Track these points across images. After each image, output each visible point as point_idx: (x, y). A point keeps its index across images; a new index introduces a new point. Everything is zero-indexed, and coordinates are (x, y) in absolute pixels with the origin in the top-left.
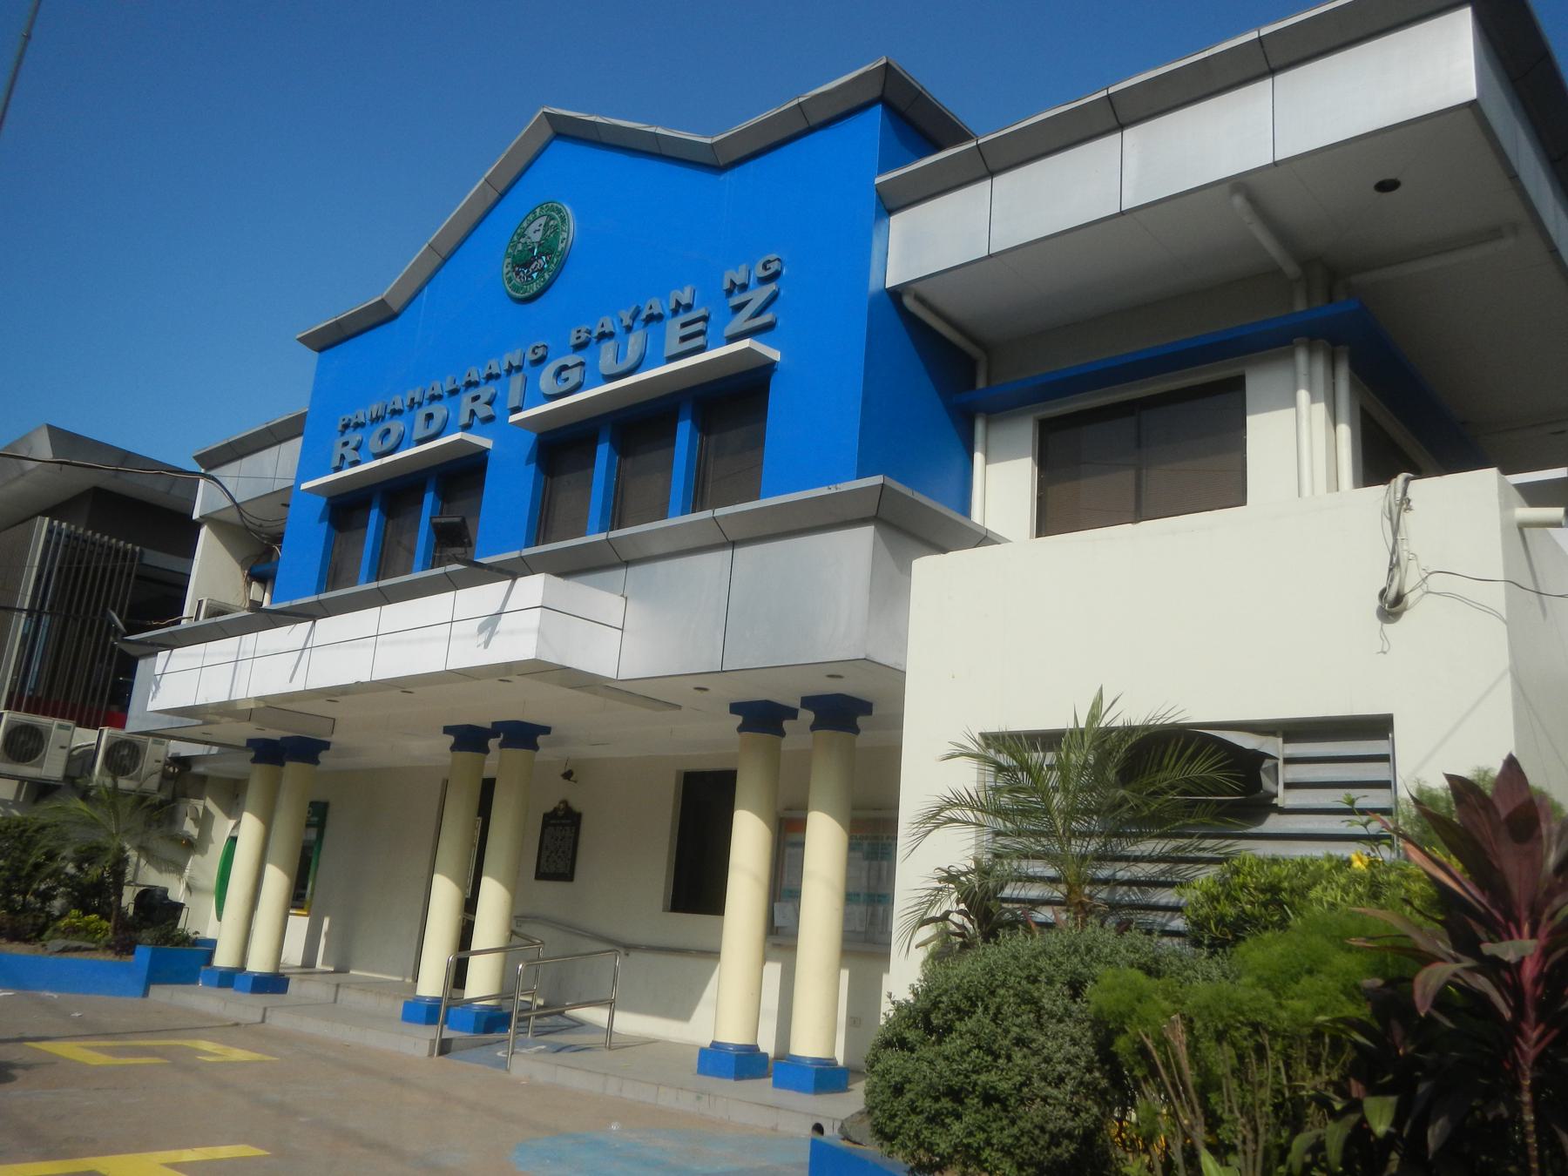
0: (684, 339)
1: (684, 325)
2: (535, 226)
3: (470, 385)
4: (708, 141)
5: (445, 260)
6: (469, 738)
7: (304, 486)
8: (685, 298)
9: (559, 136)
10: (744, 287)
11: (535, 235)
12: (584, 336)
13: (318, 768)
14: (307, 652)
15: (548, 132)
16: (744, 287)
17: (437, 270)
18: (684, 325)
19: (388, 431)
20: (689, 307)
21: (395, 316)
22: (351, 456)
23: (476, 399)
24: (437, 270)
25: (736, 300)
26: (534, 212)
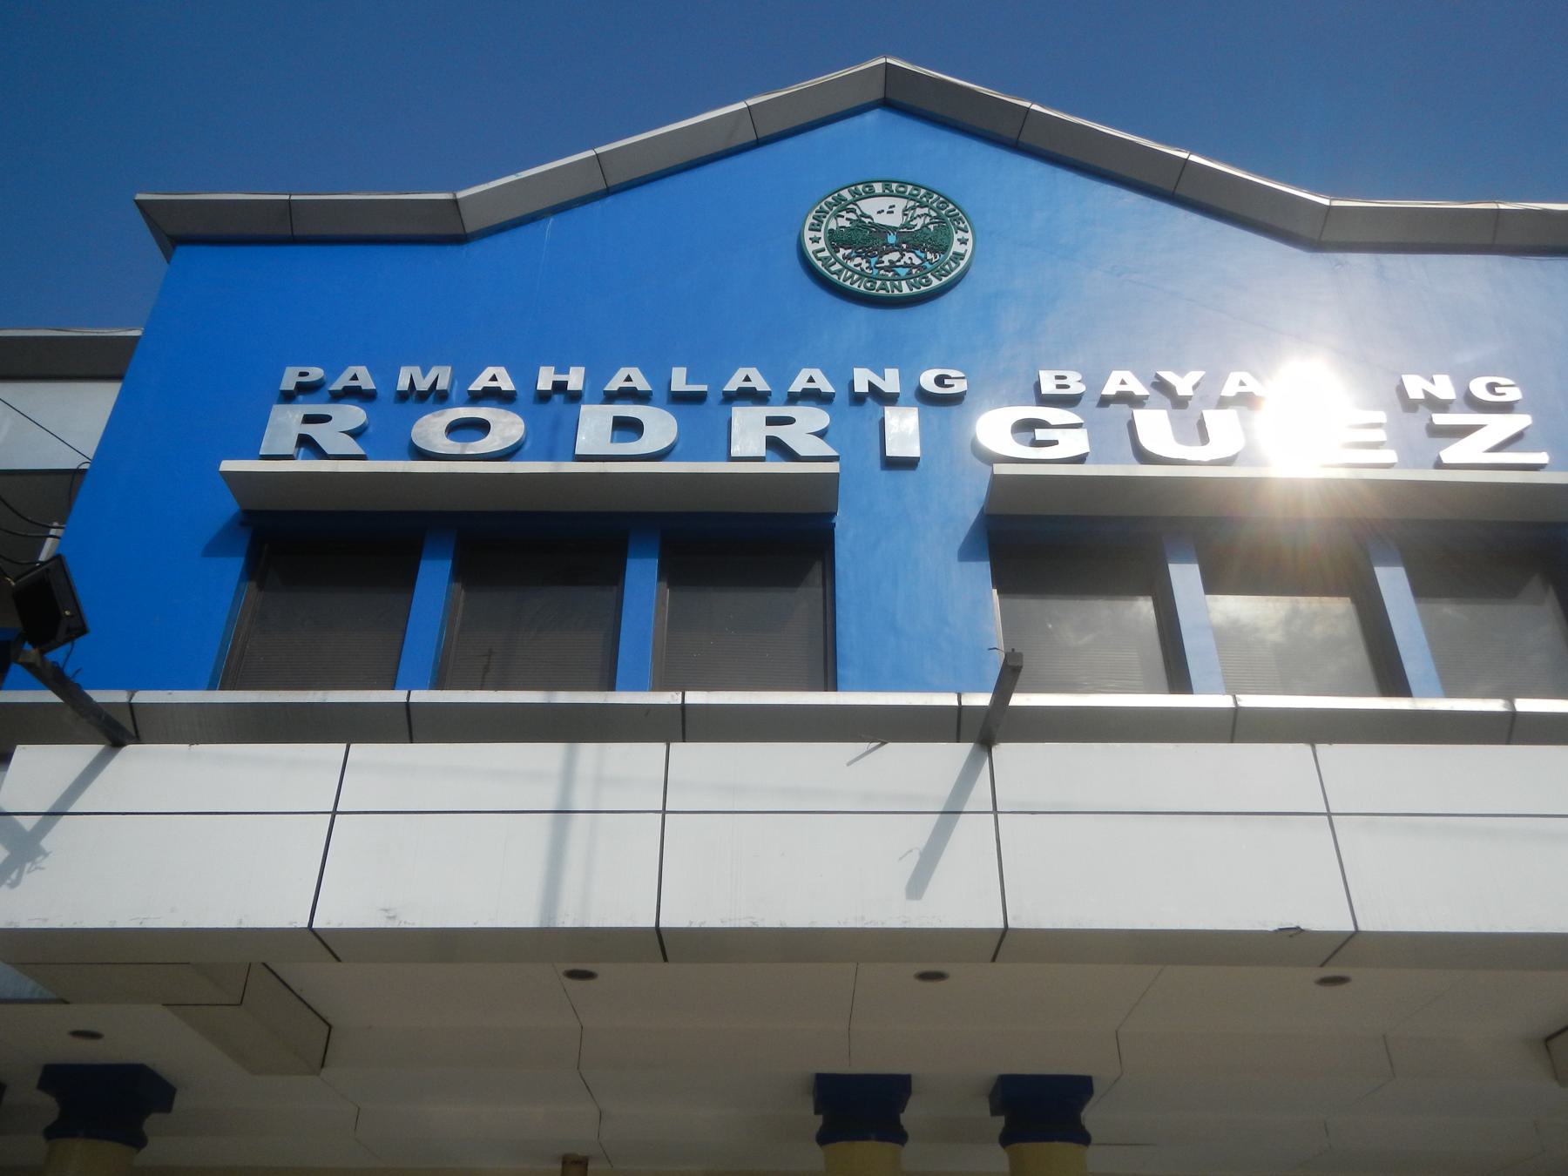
2: (884, 203)
4: (1326, 202)
5: (609, 192)
6: (859, 1106)
7: (228, 466)
9: (886, 104)
10: (1443, 406)
11: (885, 211)
13: (144, 1157)
14: (972, 832)
15: (877, 93)
16: (1443, 406)
17: (584, 200)
19: (482, 427)
21: (461, 239)
22: (328, 437)
24: (584, 200)
25: (1440, 419)
26: (868, 183)
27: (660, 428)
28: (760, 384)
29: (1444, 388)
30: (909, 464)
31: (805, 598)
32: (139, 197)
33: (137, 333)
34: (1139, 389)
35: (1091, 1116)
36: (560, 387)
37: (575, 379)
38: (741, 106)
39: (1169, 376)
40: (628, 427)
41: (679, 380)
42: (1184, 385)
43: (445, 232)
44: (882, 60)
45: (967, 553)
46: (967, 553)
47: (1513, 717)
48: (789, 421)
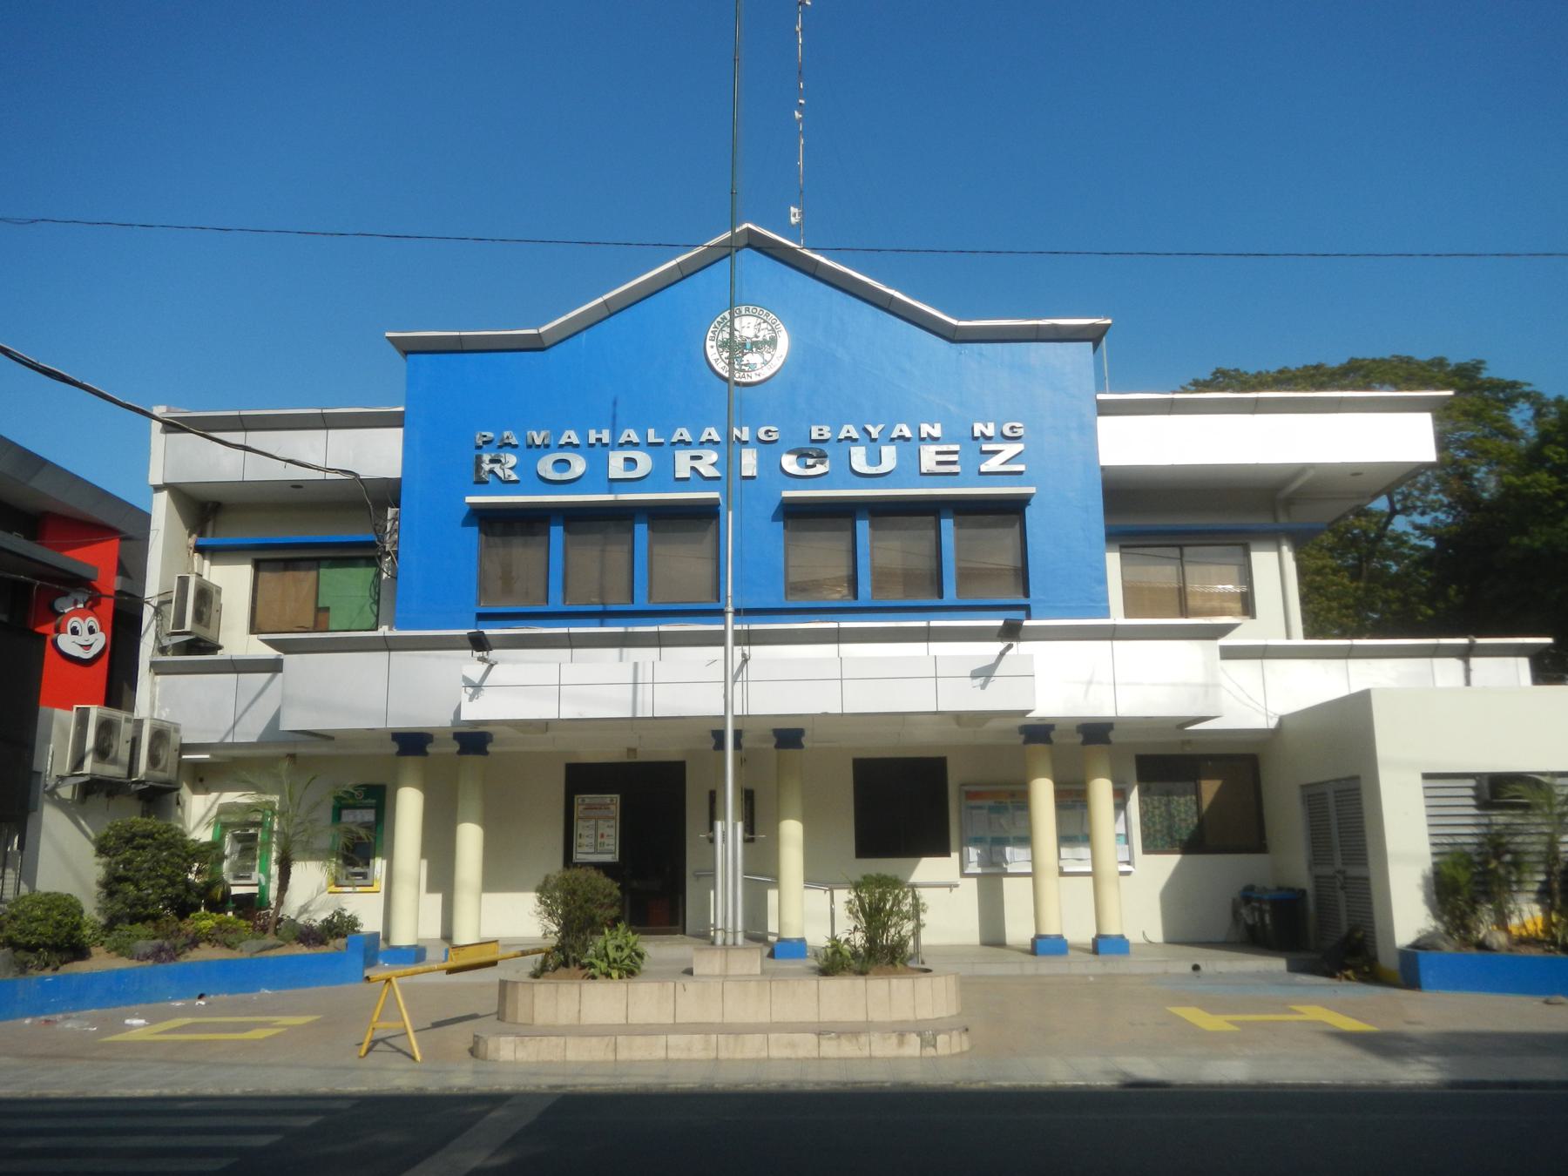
0: (939, 463)
1: (938, 453)
3: (684, 443)
4: (954, 322)
8: (936, 432)
9: (749, 246)
10: (989, 439)
12: (827, 435)
15: (743, 242)
16: (989, 439)
18: (938, 453)
20: (935, 440)
23: (694, 458)
25: (986, 447)
27: (644, 463)
28: (687, 437)
29: (990, 431)
30: (753, 478)
31: (712, 528)
32: (388, 334)
33: (401, 409)
34: (855, 435)
35: (804, 741)
36: (599, 440)
37: (606, 436)
38: (673, 263)
39: (870, 428)
40: (630, 462)
41: (652, 439)
42: (875, 433)
43: (535, 345)
44: (745, 226)
45: (775, 518)
46: (775, 518)
47: (929, 628)
48: (699, 458)
